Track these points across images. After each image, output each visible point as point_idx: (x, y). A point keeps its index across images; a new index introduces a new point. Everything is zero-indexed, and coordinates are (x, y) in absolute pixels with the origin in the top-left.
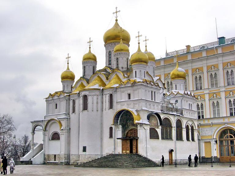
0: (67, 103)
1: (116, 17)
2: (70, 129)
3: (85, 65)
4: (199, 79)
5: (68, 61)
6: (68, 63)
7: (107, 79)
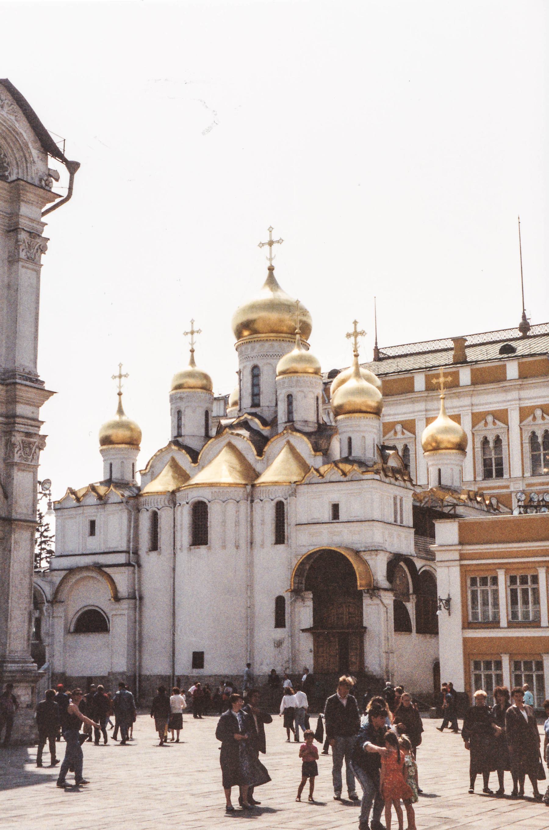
0: (130, 521)
1: (271, 259)
2: (141, 598)
3: (182, 405)
4: (495, 447)
5: (120, 387)
6: (120, 394)
7: (260, 453)
